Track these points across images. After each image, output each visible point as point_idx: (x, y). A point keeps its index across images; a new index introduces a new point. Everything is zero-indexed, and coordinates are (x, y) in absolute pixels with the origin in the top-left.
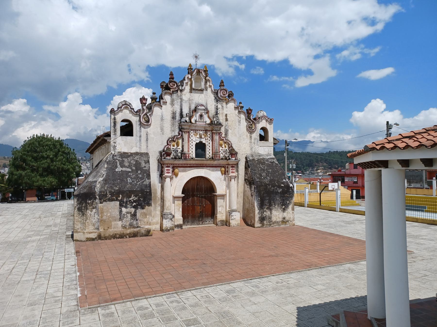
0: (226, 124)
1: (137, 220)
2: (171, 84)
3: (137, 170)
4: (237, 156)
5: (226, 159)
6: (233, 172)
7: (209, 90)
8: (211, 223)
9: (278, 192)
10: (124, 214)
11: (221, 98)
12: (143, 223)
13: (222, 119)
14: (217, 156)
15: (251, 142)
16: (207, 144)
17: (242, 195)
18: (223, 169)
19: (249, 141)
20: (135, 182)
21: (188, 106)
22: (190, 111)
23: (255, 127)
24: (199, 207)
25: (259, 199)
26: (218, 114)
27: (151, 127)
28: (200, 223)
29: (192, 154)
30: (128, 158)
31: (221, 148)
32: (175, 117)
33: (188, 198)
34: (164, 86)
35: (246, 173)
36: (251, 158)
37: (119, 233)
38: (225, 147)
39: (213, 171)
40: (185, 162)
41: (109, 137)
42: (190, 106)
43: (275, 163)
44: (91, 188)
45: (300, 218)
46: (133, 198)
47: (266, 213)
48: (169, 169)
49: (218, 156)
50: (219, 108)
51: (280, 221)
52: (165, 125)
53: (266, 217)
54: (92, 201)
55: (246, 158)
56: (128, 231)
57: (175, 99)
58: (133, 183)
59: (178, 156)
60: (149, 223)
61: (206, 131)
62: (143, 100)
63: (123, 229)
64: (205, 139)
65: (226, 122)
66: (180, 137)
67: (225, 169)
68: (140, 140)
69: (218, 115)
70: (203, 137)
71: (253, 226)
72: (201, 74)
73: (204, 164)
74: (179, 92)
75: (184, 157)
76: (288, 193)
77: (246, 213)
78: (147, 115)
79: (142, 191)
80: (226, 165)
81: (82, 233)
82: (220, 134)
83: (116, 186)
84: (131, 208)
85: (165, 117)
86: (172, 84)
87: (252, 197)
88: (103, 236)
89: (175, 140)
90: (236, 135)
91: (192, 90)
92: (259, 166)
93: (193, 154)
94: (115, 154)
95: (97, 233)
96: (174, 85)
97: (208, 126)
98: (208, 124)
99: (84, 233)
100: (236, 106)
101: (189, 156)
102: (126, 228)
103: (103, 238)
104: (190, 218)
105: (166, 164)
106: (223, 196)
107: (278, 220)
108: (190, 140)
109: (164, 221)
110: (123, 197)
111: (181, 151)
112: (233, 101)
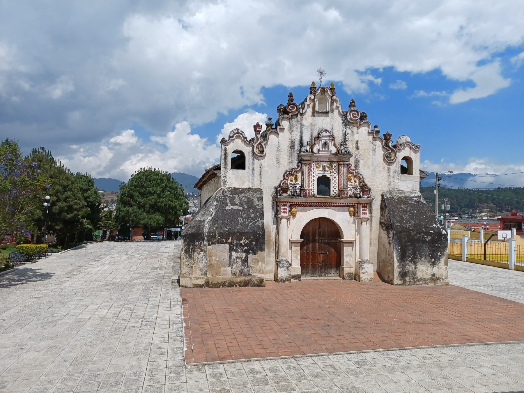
0: (357, 153)
1: (248, 267)
2: (290, 107)
3: (249, 209)
4: (370, 193)
5: (356, 196)
6: (364, 213)
7: (336, 112)
8: (336, 275)
9: (426, 240)
10: (234, 259)
11: (351, 121)
12: (255, 271)
13: (351, 147)
14: (344, 194)
15: (389, 176)
16: (331, 178)
17: (377, 242)
18: (352, 209)
19: (386, 174)
20: (247, 223)
21: (310, 132)
22: (312, 138)
23: (395, 157)
24: (321, 255)
26: (347, 141)
27: (266, 158)
28: (323, 275)
29: (313, 190)
30: (239, 195)
31: (349, 183)
32: (294, 145)
33: (307, 244)
34: (282, 110)
35: (382, 215)
36: (389, 196)
37: (228, 280)
38: (355, 182)
39: (339, 211)
40: (304, 200)
41: (220, 171)
42: (312, 133)
43: (422, 203)
44: (198, 227)
45: (455, 276)
46: (243, 241)
47: (408, 267)
48: (286, 208)
49: (346, 192)
50: (348, 134)
51: (427, 278)
52: (281, 156)
54: (199, 242)
55: (382, 196)
56: (239, 279)
57: (294, 125)
58: (244, 224)
59: (296, 193)
61: (331, 162)
62: (257, 127)
63: (233, 276)
64: (329, 172)
65: (357, 151)
66: (299, 170)
67: (355, 209)
68: (253, 174)
69: (347, 142)
70: (327, 169)
71: (391, 282)
72: (326, 94)
73: (328, 203)
74: (299, 116)
75: (303, 193)
76: (440, 243)
77: (381, 265)
78: (261, 144)
79: (254, 233)
80: (356, 204)
81: (189, 279)
82: (348, 165)
83: (226, 227)
84: (241, 252)
85: (282, 147)
86: (291, 107)
87: (390, 246)
88: (211, 282)
89: (293, 173)
90: (369, 167)
91: (315, 113)
92: (399, 206)
93: (314, 190)
94: (225, 189)
95: (204, 279)
96: (294, 108)
97: (334, 156)
98: (334, 154)
99: (191, 278)
100: (370, 131)
101: (309, 193)
102: (236, 275)
103: (211, 286)
104: (310, 267)
105: (282, 202)
106: (351, 243)
107: (425, 277)
108: (311, 173)
109: (279, 269)
110: (233, 240)
111: (300, 186)
112: (366, 125)
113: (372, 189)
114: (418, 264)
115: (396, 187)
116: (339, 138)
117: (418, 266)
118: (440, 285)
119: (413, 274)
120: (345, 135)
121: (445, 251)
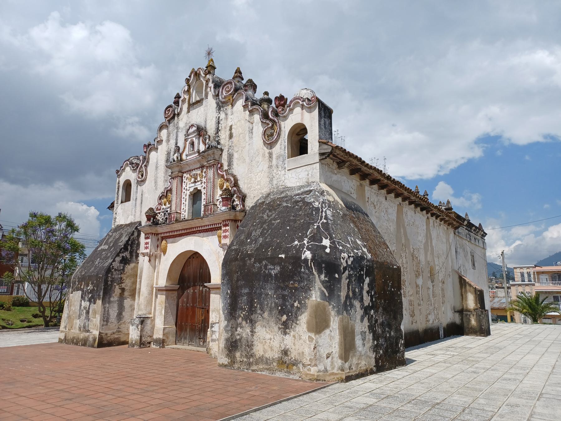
0: (230, 144)
1: (89, 321)
9: (270, 275)
13: (224, 136)
15: (270, 167)
19: (264, 166)
25: (227, 293)
27: (147, 182)
47: (241, 330)
51: (273, 359)
53: (240, 342)
60: (97, 325)
69: (219, 133)
70: (199, 179)
74: (176, 118)
76: (297, 279)
104: (188, 330)
107: (269, 355)
113: (248, 195)
114: (257, 324)
115: (281, 183)
116: (211, 130)
117: (256, 330)
118: (298, 378)
119: (248, 346)
120: (219, 123)
121: (308, 299)
